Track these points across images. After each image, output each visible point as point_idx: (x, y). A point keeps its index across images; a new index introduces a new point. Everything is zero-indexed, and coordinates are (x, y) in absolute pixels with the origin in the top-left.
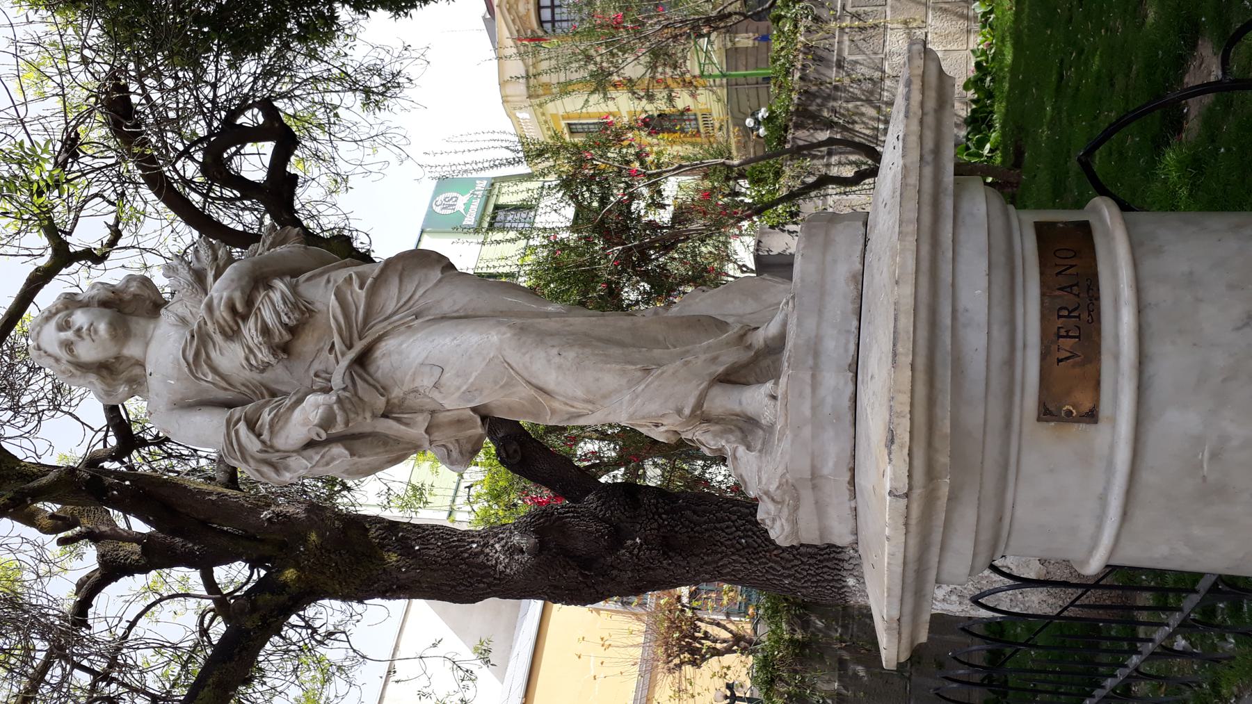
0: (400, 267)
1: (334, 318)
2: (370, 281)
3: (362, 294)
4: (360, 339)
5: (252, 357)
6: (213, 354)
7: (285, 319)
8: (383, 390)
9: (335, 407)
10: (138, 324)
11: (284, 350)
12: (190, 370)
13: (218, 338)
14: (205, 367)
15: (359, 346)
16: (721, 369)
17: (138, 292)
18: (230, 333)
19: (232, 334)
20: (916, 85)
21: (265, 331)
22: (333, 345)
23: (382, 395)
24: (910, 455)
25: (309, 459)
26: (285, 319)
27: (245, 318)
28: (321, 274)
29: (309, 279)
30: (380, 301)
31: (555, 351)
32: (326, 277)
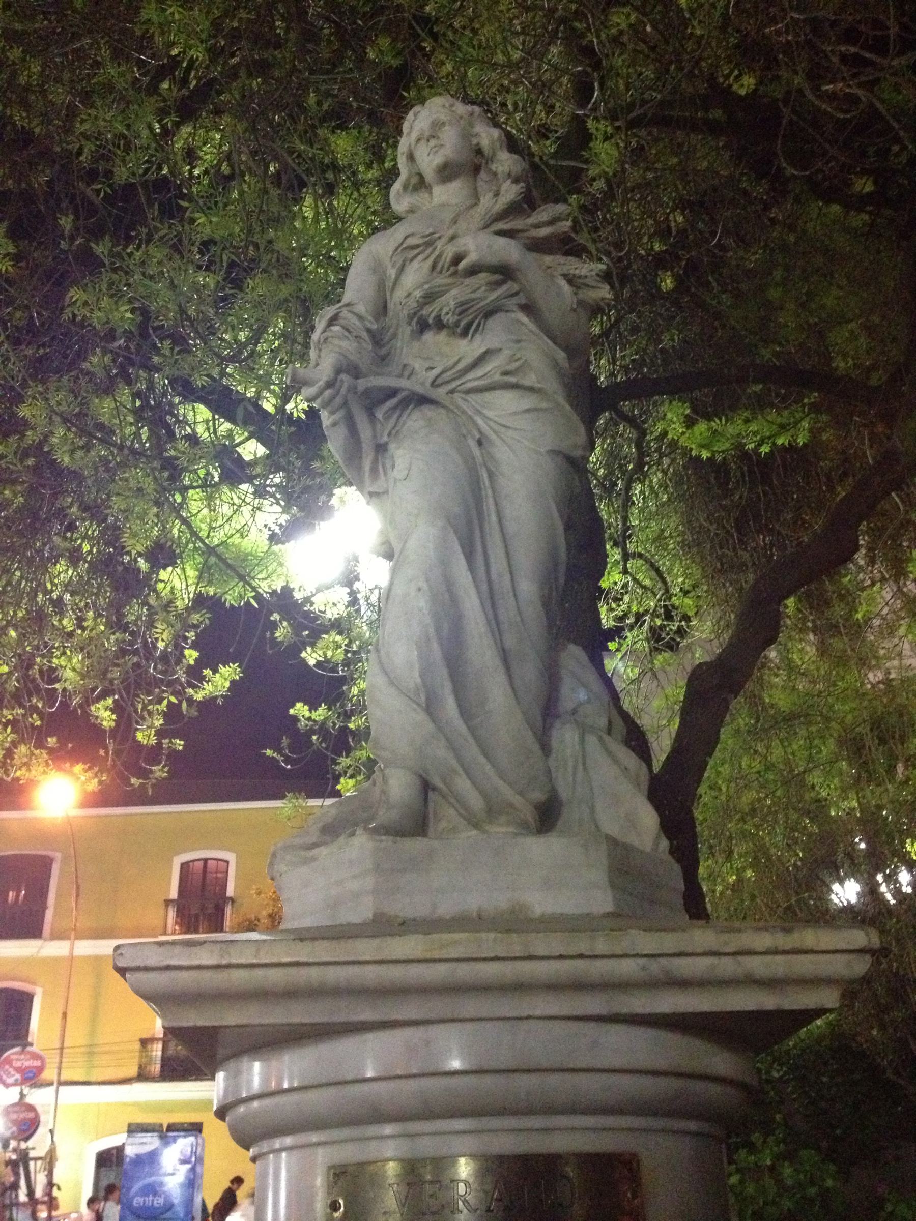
0: (544, 405)
2: (513, 380)
6: (415, 264)
18: (438, 269)
23: (389, 434)
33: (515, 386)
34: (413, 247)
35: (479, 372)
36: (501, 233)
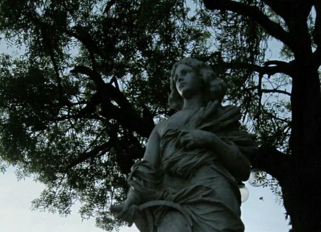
1: (184, 192)
2: (207, 199)
3: (200, 198)
4: (181, 205)
7: (178, 169)
8: (159, 223)
9: (122, 212)
10: (196, 100)
14: (164, 142)
15: (177, 206)
19: (178, 146)
23: (157, 223)
26: (178, 169)
27: (186, 150)
29: (213, 169)
30: (200, 207)
32: (219, 175)
35: (194, 196)
36: (205, 129)
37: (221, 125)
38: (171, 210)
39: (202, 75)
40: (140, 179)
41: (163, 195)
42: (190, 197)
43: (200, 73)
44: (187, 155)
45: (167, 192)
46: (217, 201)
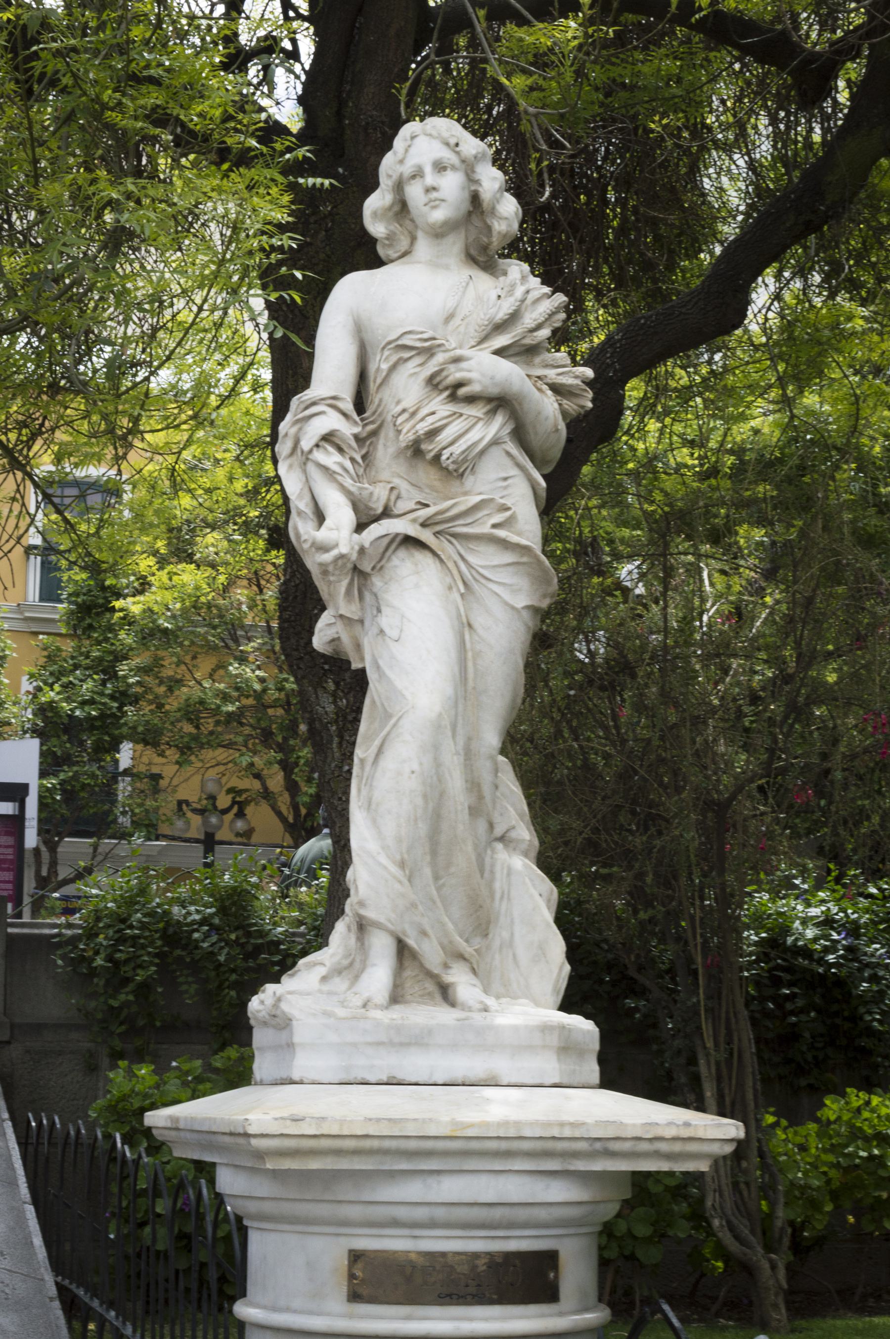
0: (525, 559)
2: (502, 533)
3: (485, 528)
4: (436, 534)
5: (405, 416)
6: (411, 364)
11: (416, 450)
12: (389, 343)
13: (432, 367)
14: (394, 358)
15: (426, 536)
16: (411, 942)
17: (495, 234)
19: (433, 383)
20: (685, 1133)
21: (432, 434)
22: (427, 506)
23: (373, 568)
24: (282, 1135)
25: (300, 496)
26: (445, 455)
27: (453, 397)
28: (519, 465)
29: (508, 453)
30: (482, 548)
31: (415, 766)
32: (515, 471)
33: (505, 544)
34: (412, 348)
35: (469, 520)
37: (528, 341)
38: (409, 541)
39: (477, 182)
40: (340, 450)
41: (389, 499)
42: (461, 522)
43: (477, 177)
44: (461, 415)
45: (395, 492)
46: (524, 542)
